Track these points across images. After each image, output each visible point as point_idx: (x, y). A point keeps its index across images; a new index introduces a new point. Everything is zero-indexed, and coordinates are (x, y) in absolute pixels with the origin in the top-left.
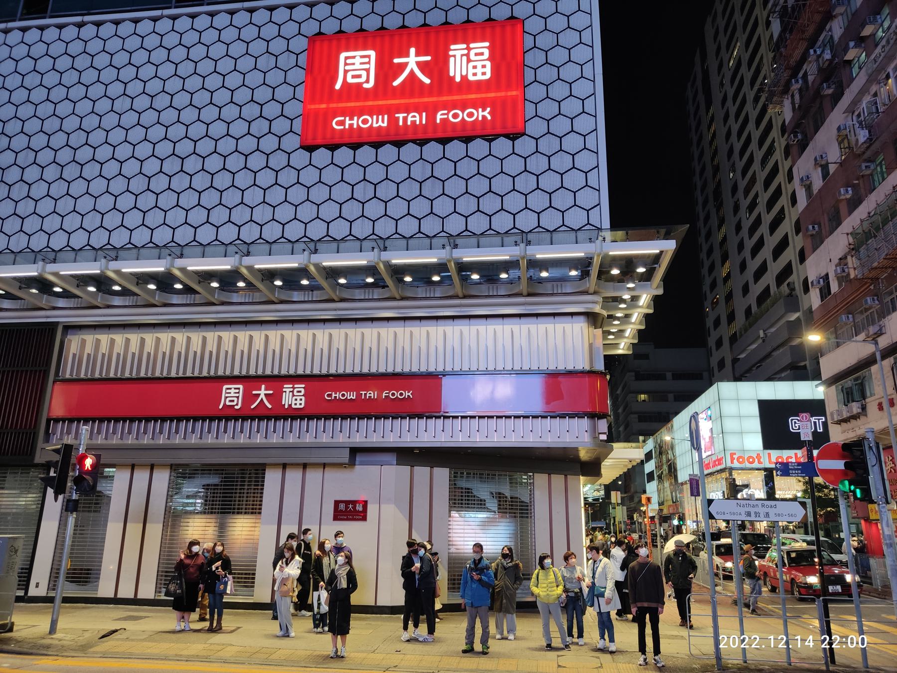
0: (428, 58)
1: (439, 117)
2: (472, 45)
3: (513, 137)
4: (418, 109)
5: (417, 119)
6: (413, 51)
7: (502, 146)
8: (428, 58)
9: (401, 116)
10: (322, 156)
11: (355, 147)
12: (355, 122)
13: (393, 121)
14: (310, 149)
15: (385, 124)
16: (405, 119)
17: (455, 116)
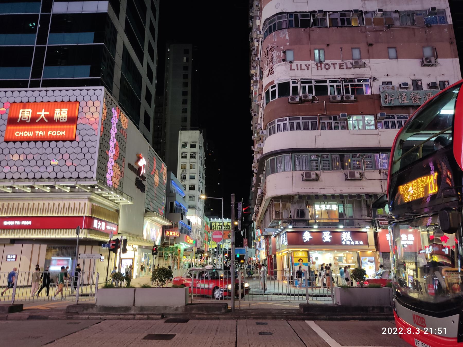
0: (48, 113)
1: (50, 133)
2: (62, 109)
3: (71, 141)
4: (42, 130)
5: (42, 134)
6: (43, 110)
7: (68, 144)
8: (48, 113)
9: (37, 132)
10: (11, 144)
11: (22, 142)
12: (22, 134)
13: (34, 134)
14: (7, 142)
15: (32, 135)
16: (38, 133)
17: (54, 133)
